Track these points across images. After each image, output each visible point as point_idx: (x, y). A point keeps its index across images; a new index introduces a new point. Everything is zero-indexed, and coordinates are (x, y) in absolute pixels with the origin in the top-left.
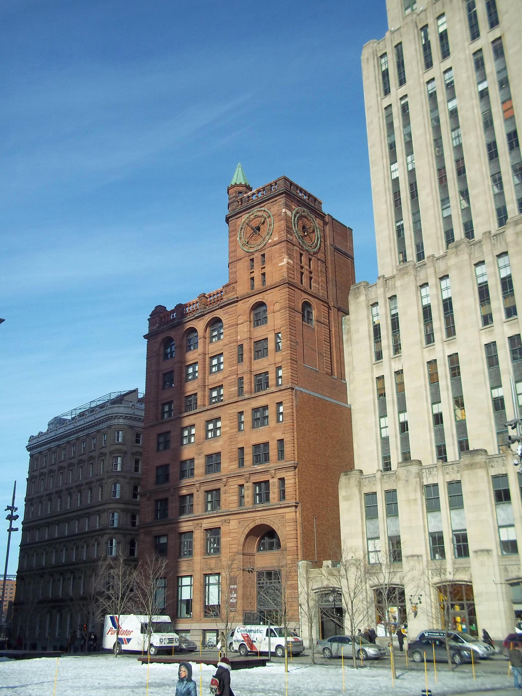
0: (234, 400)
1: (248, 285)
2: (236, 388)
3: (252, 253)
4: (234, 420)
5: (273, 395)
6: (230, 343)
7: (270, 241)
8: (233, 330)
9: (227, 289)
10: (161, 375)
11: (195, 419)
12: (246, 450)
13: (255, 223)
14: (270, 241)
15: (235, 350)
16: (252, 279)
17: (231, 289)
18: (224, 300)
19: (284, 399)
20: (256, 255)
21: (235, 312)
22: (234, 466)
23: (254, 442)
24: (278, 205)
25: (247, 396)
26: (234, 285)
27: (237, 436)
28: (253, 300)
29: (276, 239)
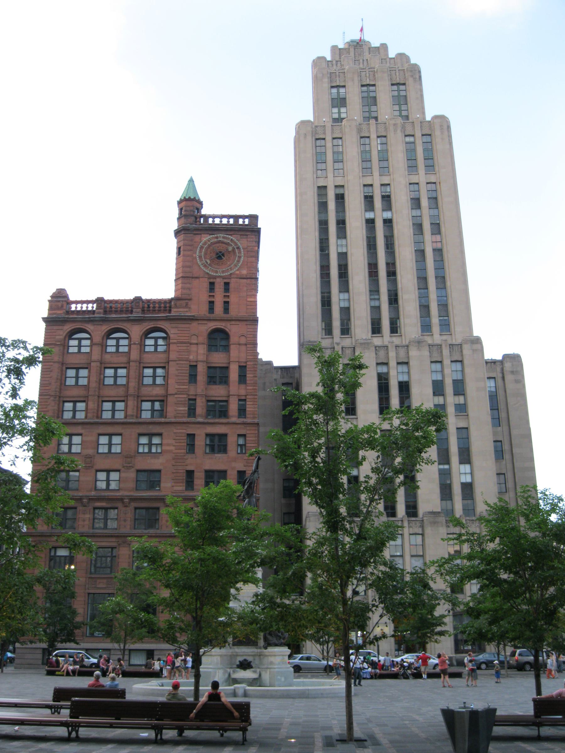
0: (185, 420)
1: (205, 307)
2: (187, 408)
3: (215, 277)
4: (182, 441)
5: (235, 426)
6: (179, 360)
7: (238, 272)
8: (185, 348)
9: (179, 303)
10: (64, 368)
12: (196, 474)
13: (222, 247)
15: (186, 370)
16: (212, 303)
17: (185, 305)
18: (173, 314)
19: (248, 432)
20: (218, 280)
21: (188, 329)
22: (181, 487)
23: (207, 467)
24: (249, 240)
25: (200, 420)
26: (187, 301)
27: (185, 457)
28: (213, 325)
29: (244, 272)
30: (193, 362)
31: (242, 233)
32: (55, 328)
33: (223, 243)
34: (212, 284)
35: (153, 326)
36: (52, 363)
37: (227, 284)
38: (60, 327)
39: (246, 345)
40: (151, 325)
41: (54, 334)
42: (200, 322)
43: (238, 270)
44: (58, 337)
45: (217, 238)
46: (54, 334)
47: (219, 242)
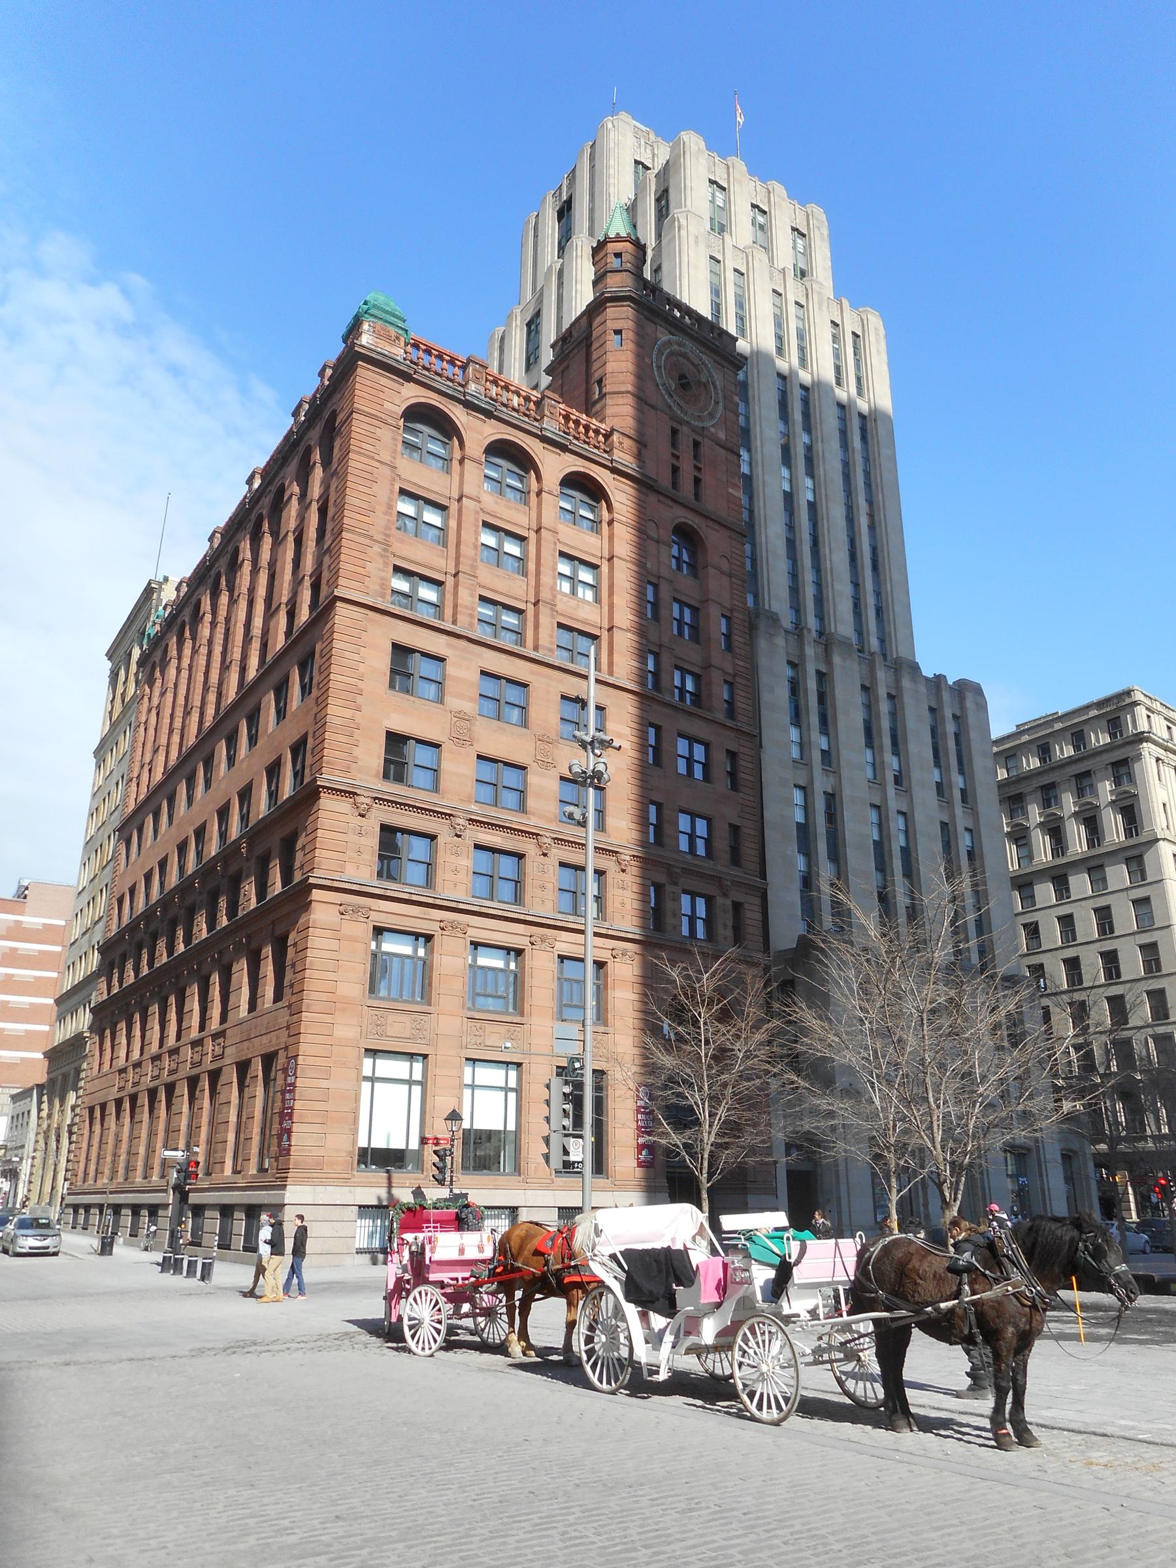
7: (712, 430)
11: (532, 672)
14: (712, 430)
19: (742, 749)
20: (685, 429)
30: (651, 574)
31: (718, 359)
32: (383, 381)
33: (688, 360)
34: (674, 432)
35: (582, 470)
36: (377, 464)
37: (696, 444)
38: (395, 386)
39: (730, 577)
40: (579, 465)
41: (381, 395)
42: (661, 498)
43: (713, 426)
44: (387, 405)
45: (680, 344)
46: (381, 395)
47: (684, 356)
